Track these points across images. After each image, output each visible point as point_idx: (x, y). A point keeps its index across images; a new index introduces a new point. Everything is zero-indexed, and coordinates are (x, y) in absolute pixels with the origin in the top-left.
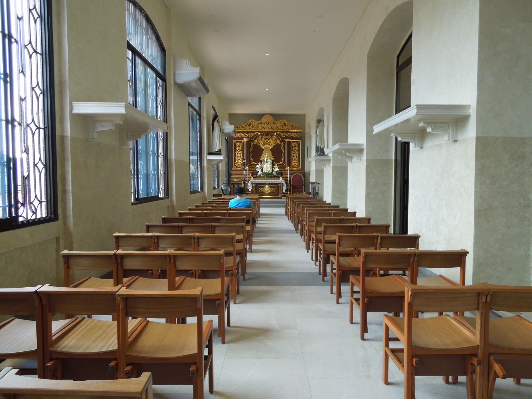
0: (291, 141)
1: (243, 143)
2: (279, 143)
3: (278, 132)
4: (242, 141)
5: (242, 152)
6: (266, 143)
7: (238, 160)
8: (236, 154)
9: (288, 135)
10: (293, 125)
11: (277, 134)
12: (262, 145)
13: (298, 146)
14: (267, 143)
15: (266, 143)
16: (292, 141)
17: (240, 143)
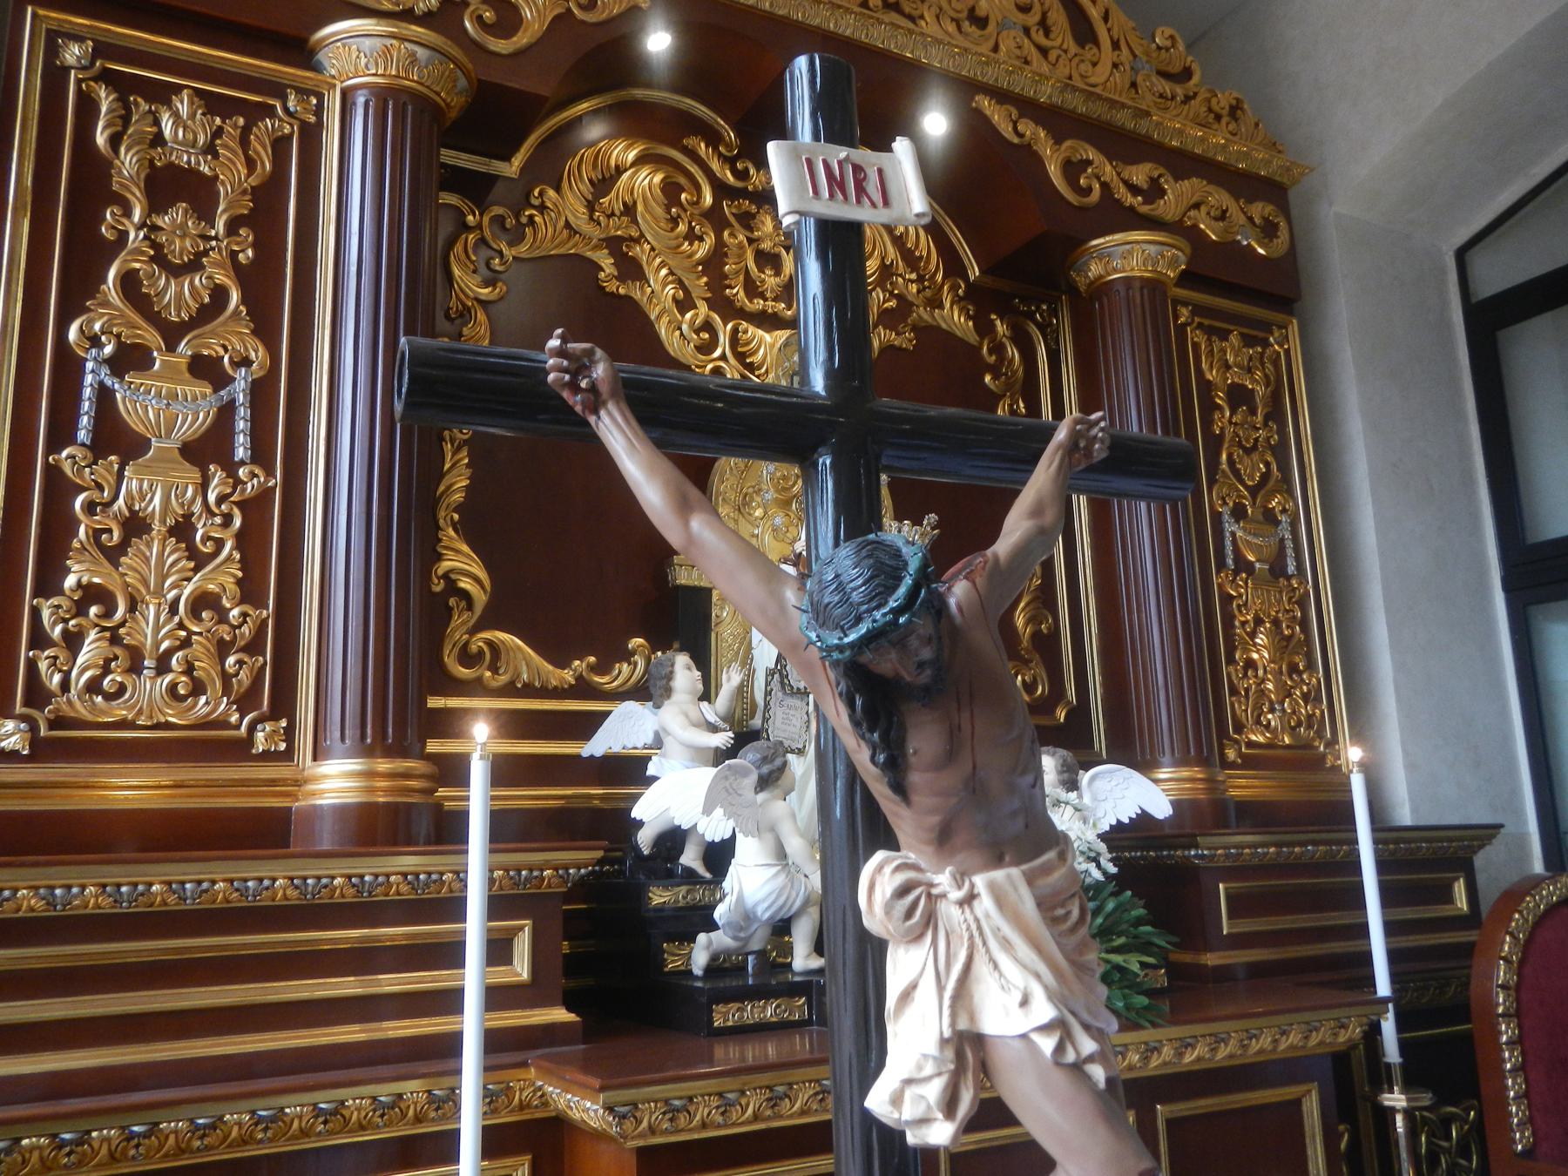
0: (1177, 302)
1: (311, 136)
2: (955, 319)
3: (1001, 96)
4: (279, 91)
5: (265, 330)
6: (752, 289)
7: (135, 525)
8: (70, 368)
9: (1134, 189)
10: (1176, 68)
11: (973, 130)
12: (684, 304)
13: (1275, 399)
14: (770, 281)
15: (752, 289)
16: (1198, 310)
17: (213, 105)
